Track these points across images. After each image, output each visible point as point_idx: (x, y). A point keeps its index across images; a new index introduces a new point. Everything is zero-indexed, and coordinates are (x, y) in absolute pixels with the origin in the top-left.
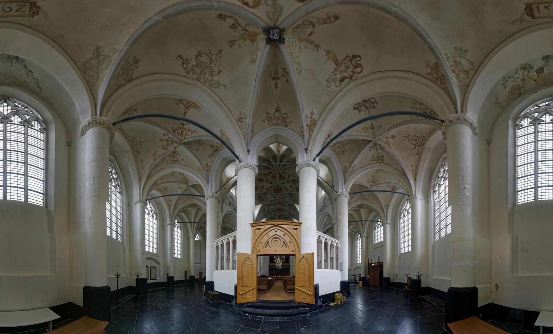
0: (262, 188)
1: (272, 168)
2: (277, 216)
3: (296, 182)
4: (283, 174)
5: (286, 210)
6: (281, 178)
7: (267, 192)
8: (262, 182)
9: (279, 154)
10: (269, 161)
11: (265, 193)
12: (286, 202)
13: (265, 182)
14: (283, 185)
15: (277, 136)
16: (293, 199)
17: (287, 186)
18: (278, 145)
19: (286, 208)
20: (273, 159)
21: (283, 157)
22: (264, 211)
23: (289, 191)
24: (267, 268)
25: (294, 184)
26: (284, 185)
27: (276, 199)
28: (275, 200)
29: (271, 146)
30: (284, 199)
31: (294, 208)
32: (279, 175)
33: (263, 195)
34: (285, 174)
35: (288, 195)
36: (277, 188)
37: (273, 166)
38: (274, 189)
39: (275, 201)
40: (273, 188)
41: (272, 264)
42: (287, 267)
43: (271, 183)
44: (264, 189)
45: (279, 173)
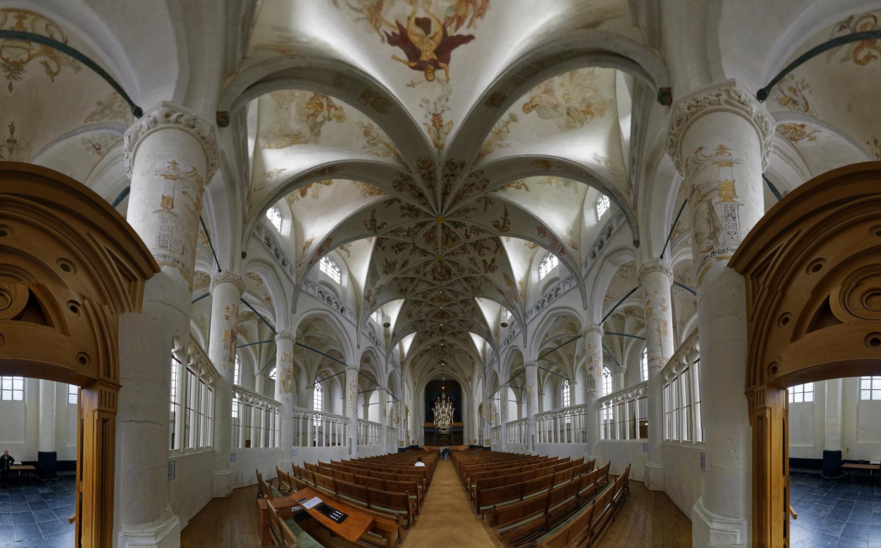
1: (424, 209)
2: (437, 331)
3: (483, 250)
4: (452, 228)
5: (456, 314)
6: (447, 240)
7: (417, 277)
11: (412, 280)
14: (452, 258)
19: (456, 309)
25: (479, 254)
26: (456, 258)
30: (451, 288)
31: (473, 309)
32: (443, 232)
39: (433, 295)
40: (429, 268)
43: (424, 253)
44: (407, 268)
45: (443, 226)
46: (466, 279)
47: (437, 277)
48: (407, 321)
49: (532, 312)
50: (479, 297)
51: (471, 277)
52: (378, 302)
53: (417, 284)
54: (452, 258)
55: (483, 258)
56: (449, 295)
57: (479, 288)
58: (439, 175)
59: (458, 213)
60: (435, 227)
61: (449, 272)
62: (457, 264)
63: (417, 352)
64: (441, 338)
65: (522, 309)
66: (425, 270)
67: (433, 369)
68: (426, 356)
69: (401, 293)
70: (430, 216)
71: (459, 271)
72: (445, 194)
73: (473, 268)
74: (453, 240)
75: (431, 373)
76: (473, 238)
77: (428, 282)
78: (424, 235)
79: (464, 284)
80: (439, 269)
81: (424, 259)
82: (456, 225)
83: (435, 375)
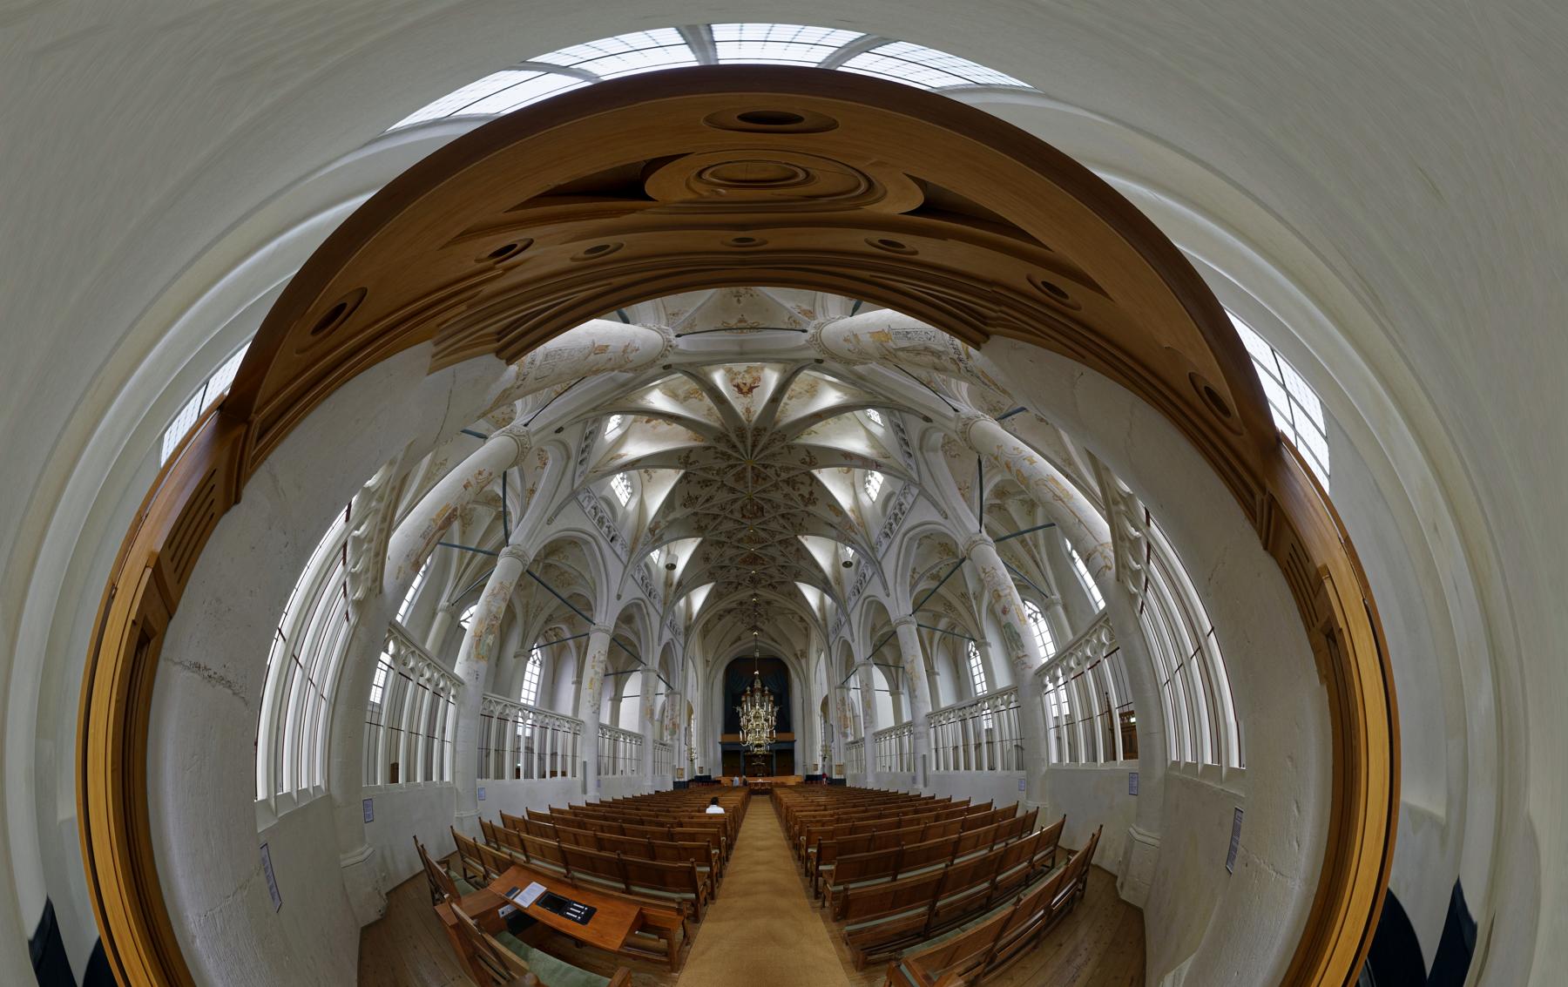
0: (707, 500)
5: (773, 559)
6: (758, 480)
11: (715, 517)
12: (773, 534)
13: (716, 488)
14: (764, 495)
16: (792, 524)
17: (777, 496)
20: (737, 435)
22: (707, 559)
23: (783, 510)
24: (716, 753)
27: (743, 526)
28: (740, 530)
30: (764, 527)
31: (798, 550)
33: (711, 523)
34: (768, 469)
38: (742, 508)
39: (741, 535)
40: (737, 505)
41: (731, 738)
42: (784, 747)
43: (733, 490)
44: (711, 504)
45: (753, 468)
46: (783, 516)
47: (747, 514)
48: (701, 568)
49: (880, 542)
50: (803, 535)
51: (788, 514)
52: (665, 538)
53: (721, 522)
54: (764, 495)
56: (763, 534)
57: (801, 524)
58: (749, 435)
59: (767, 457)
60: (745, 469)
61: (762, 509)
62: (770, 501)
63: (711, 614)
64: (752, 592)
65: (865, 540)
67: (739, 639)
68: (728, 618)
69: (698, 530)
70: (741, 460)
71: (774, 508)
72: (754, 446)
73: (789, 503)
74: (764, 479)
75: (735, 646)
76: (784, 476)
77: (735, 520)
78: (734, 475)
79: (781, 521)
80: (749, 507)
81: (732, 496)
83: (742, 648)
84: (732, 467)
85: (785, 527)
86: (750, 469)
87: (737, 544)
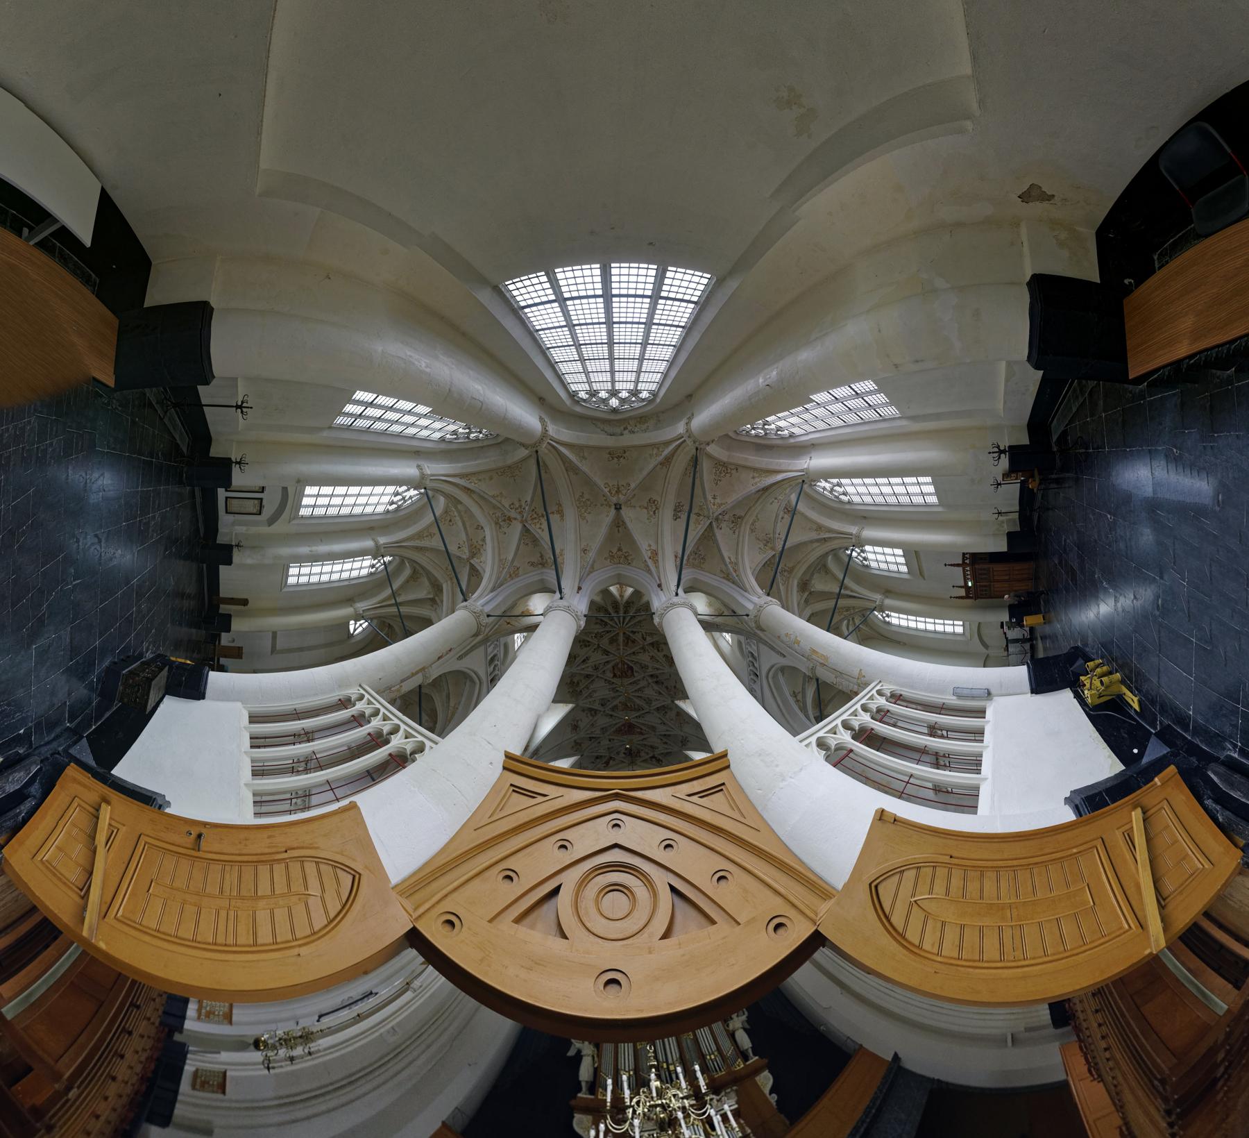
0: (584, 661)
1: (611, 623)
4: (631, 635)
5: (653, 728)
6: (628, 642)
8: (588, 648)
9: (622, 596)
10: (606, 611)
11: (588, 676)
12: (649, 701)
14: (633, 658)
15: (619, 576)
16: (667, 688)
17: (644, 658)
18: (621, 588)
19: (653, 719)
21: (629, 603)
22: (575, 727)
23: (650, 671)
25: (658, 651)
29: (612, 589)
35: (650, 681)
36: (620, 666)
37: (612, 619)
38: (614, 669)
43: (606, 653)
45: (624, 633)
55: (663, 653)
57: (675, 687)
66: (605, 668)
76: (649, 640)
82: (634, 632)
84: (608, 632)
85: (660, 693)
86: (621, 634)
87: (611, 713)
